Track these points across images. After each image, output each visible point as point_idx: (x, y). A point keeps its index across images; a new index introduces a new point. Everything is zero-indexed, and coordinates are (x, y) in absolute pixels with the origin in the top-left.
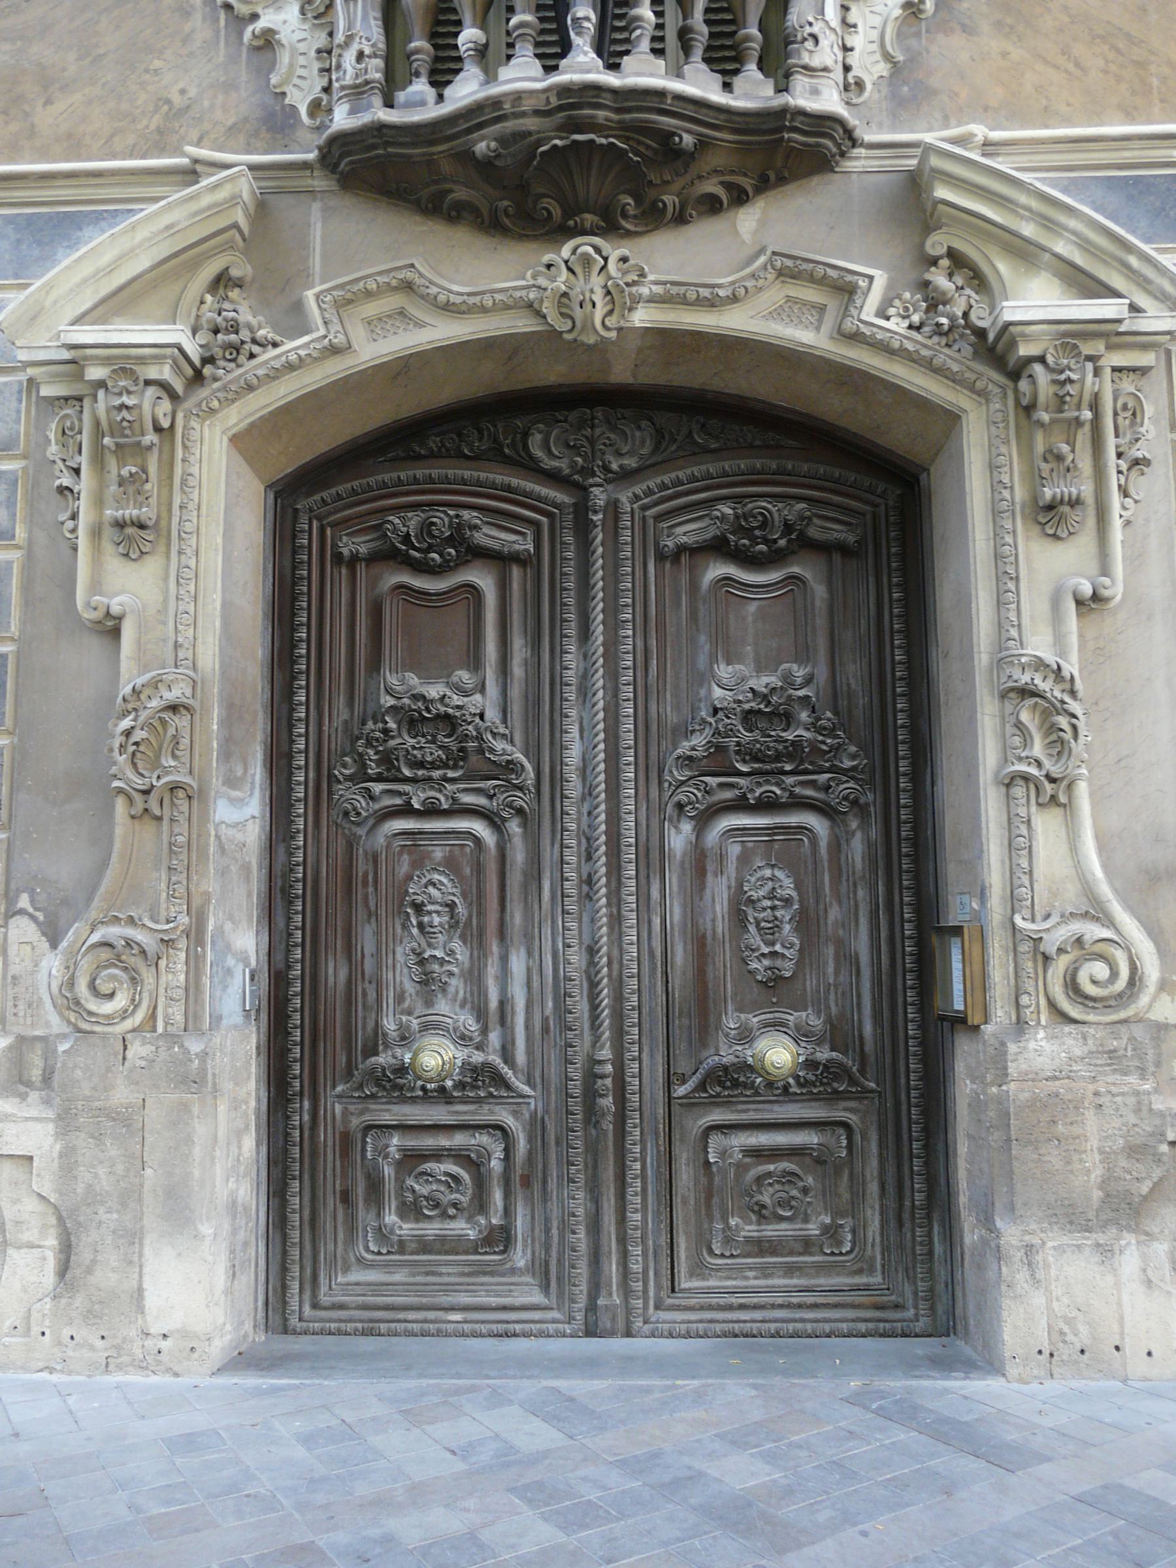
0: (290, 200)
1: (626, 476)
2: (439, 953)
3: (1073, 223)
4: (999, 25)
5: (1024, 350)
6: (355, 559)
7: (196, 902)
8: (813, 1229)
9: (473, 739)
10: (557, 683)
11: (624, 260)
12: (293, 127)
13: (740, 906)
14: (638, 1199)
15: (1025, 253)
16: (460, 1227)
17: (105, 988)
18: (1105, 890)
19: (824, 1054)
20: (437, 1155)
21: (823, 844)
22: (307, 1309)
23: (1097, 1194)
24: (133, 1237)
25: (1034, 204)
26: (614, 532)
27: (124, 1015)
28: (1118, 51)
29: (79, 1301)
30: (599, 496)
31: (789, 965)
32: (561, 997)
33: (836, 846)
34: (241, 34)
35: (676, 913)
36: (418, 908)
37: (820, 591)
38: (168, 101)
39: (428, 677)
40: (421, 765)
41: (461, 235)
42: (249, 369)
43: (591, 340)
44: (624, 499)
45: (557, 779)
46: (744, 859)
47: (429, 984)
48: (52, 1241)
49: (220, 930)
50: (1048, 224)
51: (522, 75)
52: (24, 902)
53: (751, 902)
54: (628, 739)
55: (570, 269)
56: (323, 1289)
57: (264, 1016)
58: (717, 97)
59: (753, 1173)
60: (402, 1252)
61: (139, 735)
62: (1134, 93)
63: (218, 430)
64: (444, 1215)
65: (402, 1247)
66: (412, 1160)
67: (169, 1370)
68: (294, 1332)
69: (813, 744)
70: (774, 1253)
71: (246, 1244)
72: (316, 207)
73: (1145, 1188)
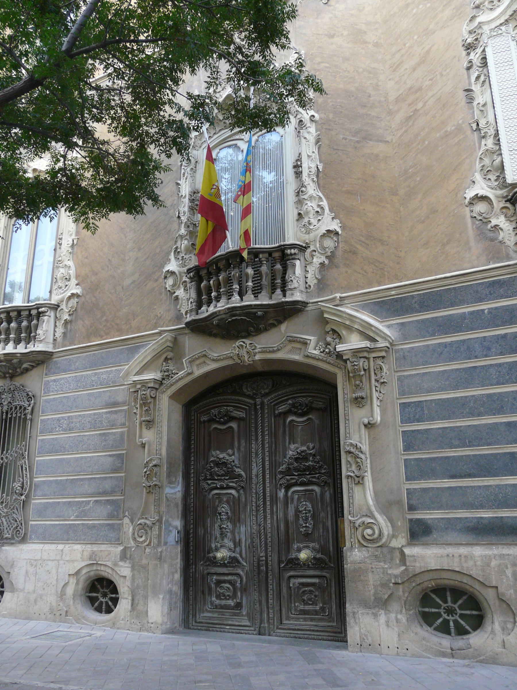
0: (181, 336)
1: (267, 395)
2: (224, 526)
3: (357, 320)
4: (345, 264)
6: (204, 422)
7: (161, 513)
8: (318, 608)
9: (231, 468)
10: (250, 452)
12: (182, 318)
13: (297, 512)
14: (272, 596)
15: (349, 328)
16: (231, 603)
17: (140, 535)
18: (373, 508)
19: (319, 556)
20: (225, 582)
21: (318, 494)
22: (194, 622)
23: (373, 598)
24: (146, 597)
25: (347, 316)
27: (145, 541)
28: (376, 266)
29: (135, 613)
30: (258, 401)
31: (311, 530)
32: (252, 538)
33: (322, 495)
35: (281, 514)
36: (220, 514)
37: (317, 422)
38: (157, 316)
39: (222, 451)
40: (219, 476)
41: (218, 340)
42: (172, 380)
44: (266, 401)
45: (251, 479)
46: (299, 499)
47: (223, 535)
48: (130, 598)
49: (167, 521)
53: (300, 512)
54: (267, 467)
55: (239, 348)
56: (197, 618)
57: (182, 543)
59: (301, 591)
60: (216, 608)
61: (148, 473)
62: (380, 277)
63: (166, 396)
64: (226, 599)
65: (216, 607)
66: (219, 583)
67: (153, 632)
68: (191, 629)
69: (313, 466)
70: (308, 615)
71: (176, 603)
72: (187, 337)
73: (386, 597)
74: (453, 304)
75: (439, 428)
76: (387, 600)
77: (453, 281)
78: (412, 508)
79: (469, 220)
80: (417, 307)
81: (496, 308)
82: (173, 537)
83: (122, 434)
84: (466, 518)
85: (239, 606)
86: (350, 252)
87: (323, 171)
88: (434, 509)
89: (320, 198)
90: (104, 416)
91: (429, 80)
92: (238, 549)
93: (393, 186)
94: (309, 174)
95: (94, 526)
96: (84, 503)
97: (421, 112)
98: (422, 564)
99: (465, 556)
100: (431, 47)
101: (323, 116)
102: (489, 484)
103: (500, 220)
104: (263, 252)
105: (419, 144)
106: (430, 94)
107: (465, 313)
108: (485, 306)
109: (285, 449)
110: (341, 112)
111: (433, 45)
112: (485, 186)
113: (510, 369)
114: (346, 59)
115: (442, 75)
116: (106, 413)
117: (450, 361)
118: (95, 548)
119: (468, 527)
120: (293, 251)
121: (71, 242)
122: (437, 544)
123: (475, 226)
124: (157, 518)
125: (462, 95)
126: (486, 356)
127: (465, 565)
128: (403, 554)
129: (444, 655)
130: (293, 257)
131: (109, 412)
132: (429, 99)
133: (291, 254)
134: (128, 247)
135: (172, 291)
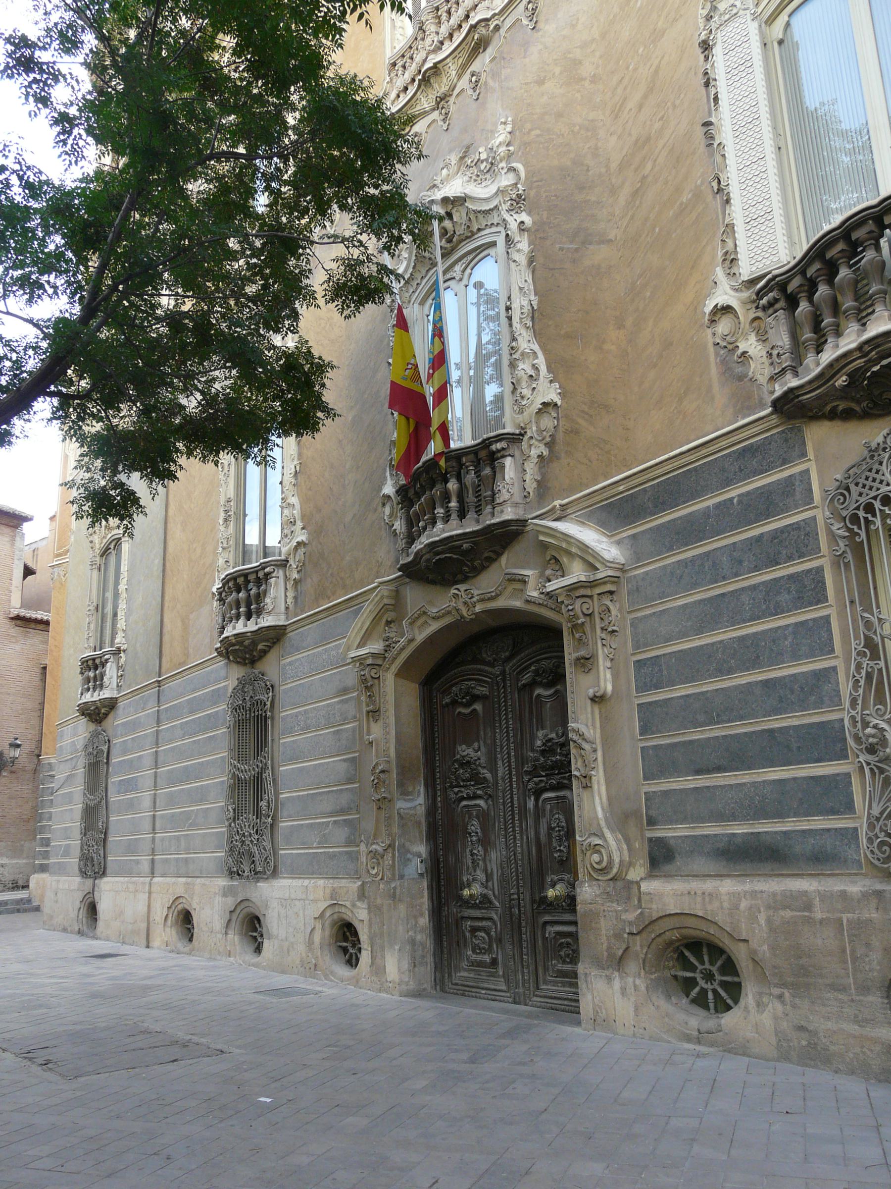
1: (508, 659)
6: (447, 705)
18: (603, 823)
23: (605, 954)
24: (382, 948)
31: (565, 855)
35: (532, 834)
36: (470, 834)
41: (438, 587)
42: (394, 652)
45: (497, 783)
49: (402, 846)
61: (376, 781)
66: (474, 930)
70: (567, 977)
71: (423, 957)
73: (620, 953)
74: (695, 494)
76: (621, 958)
77: (692, 458)
79: (711, 349)
81: (748, 493)
82: (416, 867)
84: (715, 835)
85: (494, 962)
86: (572, 432)
87: (539, 308)
88: (677, 823)
92: (490, 884)
94: (521, 319)
98: (660, 906)
99: (710, 894)
100: (660, 62)
101: (537, 217)
102: (743, 781)
103: (749, 343)
107: (709, 507)
108: (733, 493)
109: (533, 738)
110: (556, 206)
112: (727, 288)
113: (767, 593)
114: (560, 115)
115: (674, 106)
116: (339, 702)
117: (692, 588)
118: (336, 884)
119: (718, 849)
120: (499, 446)
121: (293, 470)
122: (682, 876)
124: (388, 842)
126: (736, 575)
127: (709, 907)
129: (688, 1039)
130: (502, 453)
132: (660, 152)
134: (347, 467)
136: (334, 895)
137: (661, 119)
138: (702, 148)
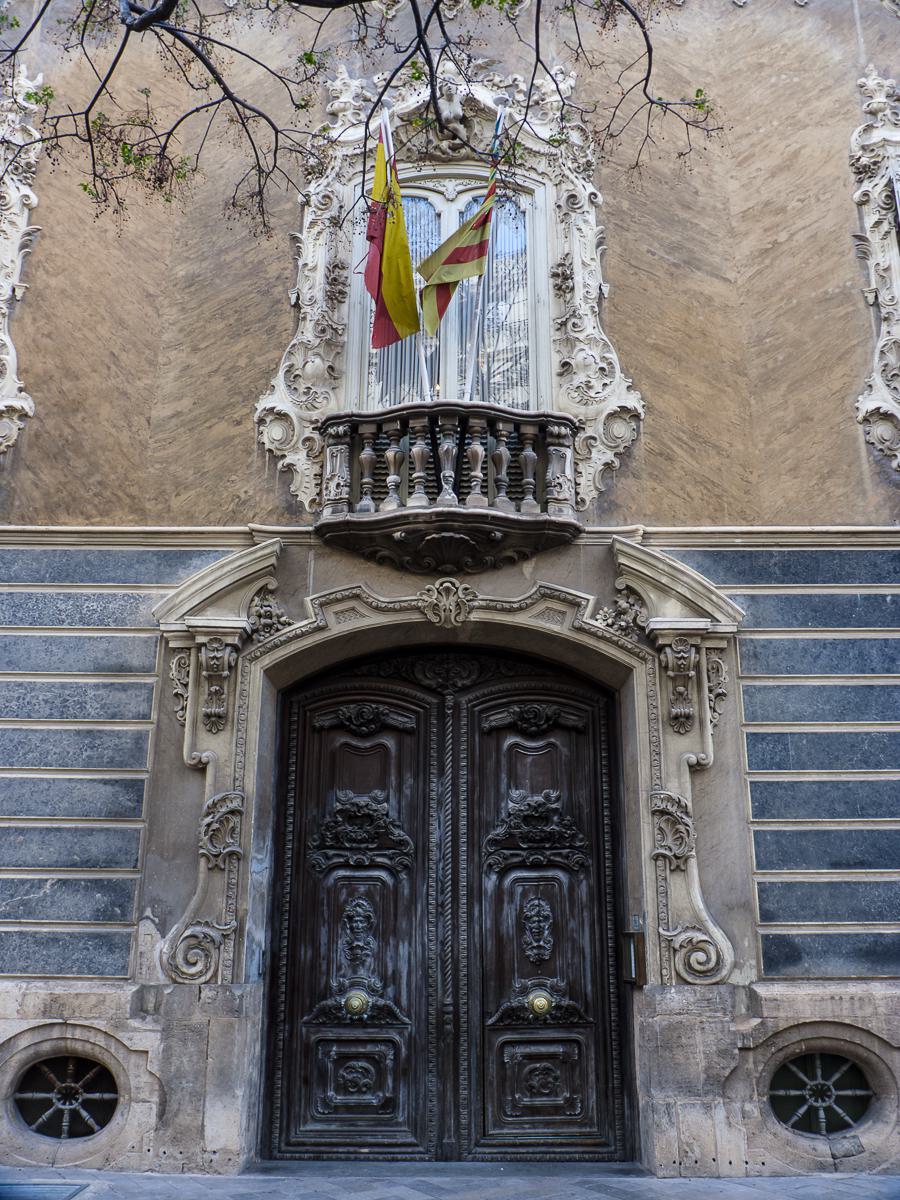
1: (465, 689)
2: (361, 944)
3: (685, 579)
4: (651, 475)
5: (661, 641)
6: (322, 728)
7: (241, 913)
8: (560, 1101)
9: (382, 828)
10: (426, 798)
11: (466, 589)
12: (301, 512)
13: (522, 921)
14: (466, 1082)
16: (371, 1099)
17: (192, 960)
18: (704, 915)
19: (566, 1002)
20: (357, 1057)
21: (565, 887)
22: (283, 1145)
23: (703, 1076)
24: (199, 1097)
26: (456, 717)
27: (201, 974)
29: (170, 1132)
30: (450, 700)
32: (426, 968)
33: (571, 888)
34: (276, 465)
35: (488, 923)
36: (350, 918)
37: (565, 751)
38: (238, 497)
39: (359, 792)
40: (354, 841)
41: (385, 571)
43: (449, 626)
45: (426, 851)
46: (524, 895)
47: (356, 961)
48: (155, 1099)
50: (673, 577)
51: (417, 503)
52: (148, 912)
53: (528, 918)
54: (463, 830)
56: (293, 1134)
57: (268, 978)
58: (513, 516)
59: (527, 1069)
60: (336, 1112)
62: (716, 510)
63: (259, 667)
64: (360, 1092)
65: (336, 1109)
67: (215, 1172)
68: (276, 1159)
69: (560, 833)
70: (540, 1115)
73: (727, 1073)
74: (836, 579)
75: (814, 782)
76: (727, 1078)
77: (839, 541)
78: (767, 916)
79: (863, 447)
80: (778, 572)
82: (253, 965)
83: (139, 738)
84: (857, 935)
85: (389, 1105)
86: (661, 454)
87: (611, 299)
88: (805, 918)
89: (605, 344)
90: (91, 693)
91: (799, 200)
92: (390, 991)
93: (738, 358)
94: (585, 297)
95: (54, 939)
96: (27, 886)
97: (785, 248)
98: (790, 1015)
99: (860, 999)
100: (800, 149)
101: (609, 199)
102: (893, 879)
104: (506, 421)
105: (782, 299)
106: (800, 223)
107: (856, 596)
109: (499, 798)
110: (645, 204)
111: (804, 147)
116: (96, 686)
117: (832, 672)
118: (59, 988)
119: (861, 950)
120: (563, 430)
121: (7, 293)
122: (808, 979)
123: (871, 458)
124: (234, 923)
125: (850, 242)
126: (888, 671)
127: (859, 1013)
128: (753, 997)
129: (822, 1167)
130: (561, 441)
131: (105, 686)
133: (559, 436)
134: (165, 337)
135: (279, 453)
136: (52, 1006)
137: (802, 201)
138: (852, 255)
